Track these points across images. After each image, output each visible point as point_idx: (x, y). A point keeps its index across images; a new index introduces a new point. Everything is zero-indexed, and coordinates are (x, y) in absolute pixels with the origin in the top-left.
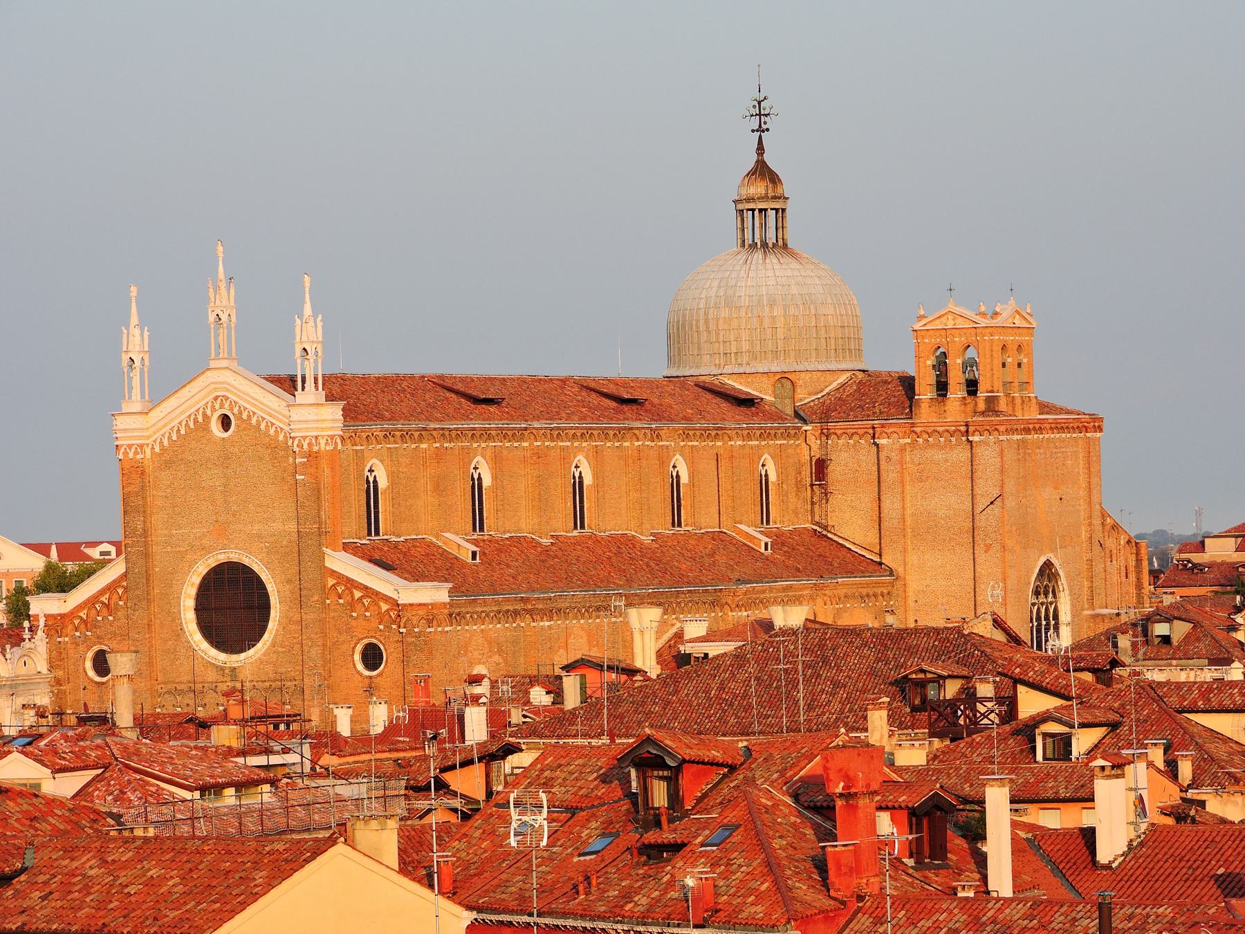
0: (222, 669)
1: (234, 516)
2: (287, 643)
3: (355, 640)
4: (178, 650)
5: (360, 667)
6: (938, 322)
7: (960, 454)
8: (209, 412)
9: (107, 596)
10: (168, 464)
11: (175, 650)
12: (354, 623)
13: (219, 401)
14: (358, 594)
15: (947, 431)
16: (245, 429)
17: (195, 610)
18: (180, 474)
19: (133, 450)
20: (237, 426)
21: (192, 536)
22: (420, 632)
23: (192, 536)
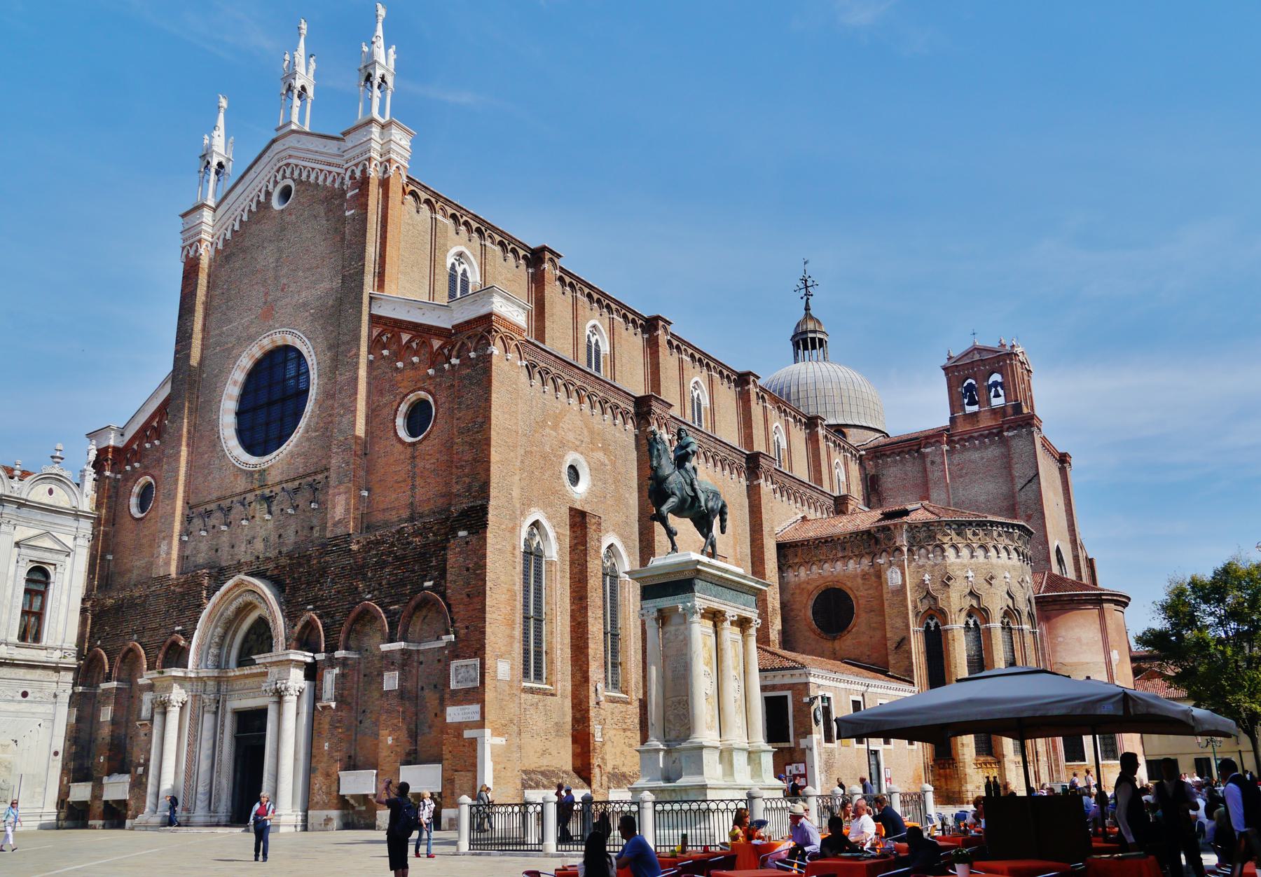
0: (251, 474)
1: (282, 290)
2: (322, 425)
3: (398, 400)
4: (212, 463)
5: (403, 434)
6: (965, 358)
7: (993, 452)
8: (271, 187)
9: (157, 420)
10: (228, 258)
11: (210, 464)
12: (399, 377)
13: (281, 172)
15: (981, 435)
17: (236, 414)
18: (237, 265)
20: (297, 191)
21: (240, 327)
23: (240, 327)
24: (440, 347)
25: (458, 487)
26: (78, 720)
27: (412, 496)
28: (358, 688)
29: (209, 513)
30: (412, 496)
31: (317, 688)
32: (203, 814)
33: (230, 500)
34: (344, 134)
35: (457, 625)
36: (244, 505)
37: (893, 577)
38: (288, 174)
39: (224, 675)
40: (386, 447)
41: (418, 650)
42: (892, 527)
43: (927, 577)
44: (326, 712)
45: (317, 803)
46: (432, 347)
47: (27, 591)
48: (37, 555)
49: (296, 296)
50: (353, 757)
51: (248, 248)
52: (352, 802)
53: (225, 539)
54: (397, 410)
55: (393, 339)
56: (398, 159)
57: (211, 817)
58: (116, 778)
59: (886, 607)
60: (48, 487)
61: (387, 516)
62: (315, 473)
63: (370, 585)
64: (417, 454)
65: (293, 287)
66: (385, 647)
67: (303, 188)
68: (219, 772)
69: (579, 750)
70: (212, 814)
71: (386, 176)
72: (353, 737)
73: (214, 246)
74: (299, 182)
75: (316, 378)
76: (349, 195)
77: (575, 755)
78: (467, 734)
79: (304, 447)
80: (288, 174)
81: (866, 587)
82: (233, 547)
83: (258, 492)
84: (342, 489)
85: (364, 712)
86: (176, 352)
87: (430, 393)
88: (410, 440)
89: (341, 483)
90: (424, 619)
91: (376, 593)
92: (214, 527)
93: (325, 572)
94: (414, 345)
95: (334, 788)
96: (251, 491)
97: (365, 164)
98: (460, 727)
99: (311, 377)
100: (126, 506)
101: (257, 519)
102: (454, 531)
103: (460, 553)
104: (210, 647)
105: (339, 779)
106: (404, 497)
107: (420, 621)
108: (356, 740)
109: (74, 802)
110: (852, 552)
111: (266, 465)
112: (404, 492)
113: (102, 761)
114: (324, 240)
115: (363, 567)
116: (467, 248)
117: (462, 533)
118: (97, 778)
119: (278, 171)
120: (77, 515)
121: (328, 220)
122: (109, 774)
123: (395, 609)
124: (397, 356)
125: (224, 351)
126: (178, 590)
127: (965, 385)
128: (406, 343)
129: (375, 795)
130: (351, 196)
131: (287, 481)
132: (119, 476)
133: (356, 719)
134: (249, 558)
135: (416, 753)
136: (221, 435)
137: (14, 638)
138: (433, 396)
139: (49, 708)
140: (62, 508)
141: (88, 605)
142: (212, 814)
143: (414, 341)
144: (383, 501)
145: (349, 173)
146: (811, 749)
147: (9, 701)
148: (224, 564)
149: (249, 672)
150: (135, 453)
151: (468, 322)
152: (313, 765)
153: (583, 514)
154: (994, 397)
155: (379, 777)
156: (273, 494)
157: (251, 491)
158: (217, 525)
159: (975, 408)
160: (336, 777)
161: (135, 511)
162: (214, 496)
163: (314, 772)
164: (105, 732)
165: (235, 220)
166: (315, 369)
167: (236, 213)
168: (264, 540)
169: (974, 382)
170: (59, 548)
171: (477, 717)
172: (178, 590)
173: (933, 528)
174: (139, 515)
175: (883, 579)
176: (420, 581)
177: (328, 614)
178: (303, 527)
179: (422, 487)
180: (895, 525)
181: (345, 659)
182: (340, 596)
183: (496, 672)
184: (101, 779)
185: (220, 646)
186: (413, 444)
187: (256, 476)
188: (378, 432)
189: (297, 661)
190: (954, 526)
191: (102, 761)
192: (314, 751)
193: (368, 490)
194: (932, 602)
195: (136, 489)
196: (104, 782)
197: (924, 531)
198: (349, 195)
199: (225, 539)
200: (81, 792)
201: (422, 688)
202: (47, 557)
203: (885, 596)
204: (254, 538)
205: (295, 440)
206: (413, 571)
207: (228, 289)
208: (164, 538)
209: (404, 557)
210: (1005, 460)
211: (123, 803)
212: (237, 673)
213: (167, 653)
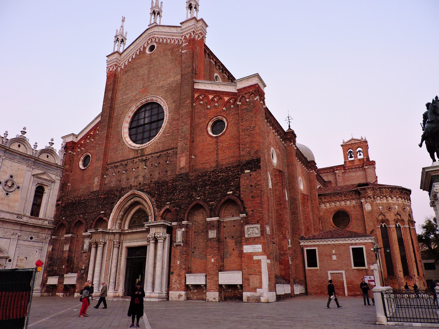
0: (136, 151)
1: (151, 82)
3: (208, 121)
5: (211, 133)
8: (145, 45)
9: (93, 132)
10: (126, 72)
11: (117, 147)
12: (208, 111)
13: (150, 40)
14: (211, 97)
16: (160, 47)
18: (130, 74)
19: (112, 68)
20: (157, 47)
21: (132, 96)
22: (250, 102)
23: (132, 96)
24: (229, 99)
25: (243, 153)
26: (53, 249)
27: (217, 158)
28: (192, 237)
29: (116, 167)
30: (217, 158)
31: (173, 237)
32: (112, 291)
33: (126, 161)
34: (181, 24)
35: (247, 210)
36: (133, 163)
37: (368, 207)
38: (153, 40)
39: (123, 232)
40: (203, 139)
41: (223, 221)
42: (367, 189)
43: (381, 207)
44: (178, 248)
45: (174, 288)
46: (224, 99)
47: (35, 196)
48: (40, 181)
49: (158, 84)
50: (190, 268)
51: (135, 68)
52: (192, 288)
53: (124, 176)
54: (208, 124)
55: (205, 97)
56: (203, 34)
57: (115, 293)
58: (70, 275)
59: (365, 218)
60: (47, 154)
61: (204, 166)
62: (168, 150)
63: (199, 193)
64: (219, 141)
65: (156, 81)
66: (208, 219)
67: (160, 45)
68: (119, 273)
69: (283, 267)
70: (116, 292)
71: (199, 39)
72: (190, 259)
73: (120, 68)
74: (158, 43)
75: (168, 114)
76: (184, 45)
77: (281, 269)
78: (255, 258)
79: (163, 140)
80: (153, 40)
81: (355, 211)
82: (128, 180)
83: (139, 158)
84: (184, 154)
85: (195, 248)
86: (103, 106)
87: (224, 117)
88: (215, 136)
89: (183, 152)
90: (226, 208)
91: (202, 197)
92: (119, 172)
93: (176, 188)
94: (216, 99)
95: (183, 281)
96: (136, 158)
97: (191, 34)
98: (250, 255)
99: (165, 113)
100: (78, 164)
101: (140, 168)
102: (243, 171)
103: (247, 179)
104: (117, 220)
105: (186, 277)
106: (213, 158)
107: (224, 209)
108: (191, 260)
109: (49, 285)
110: (349, 198)
111: (144, 147)
112: (213, 156)
113: (64, 267)
114: (170, 63)
115: (195, 186)
116: (219, 75)
117: (247, 171)
118: (61, 275)
119: (149, 40)
120: (57, 166)
121: (172, 56)
122: (66, 273)
123: (213, 203)
124: (207, 104)
125: (124, 105)
126: (102, 196)
127: (349, 151)
128: (211, 99)
129: (205, 285)
130: (185, 46)
131: (154, 153)
132: (74, 153)
133: (191, 252)
134: (136, 184)
135: (224, 266)
136: (123, 136)
137: (29, 214)
138: (226, 118)
139: (40, 245)
140: (51, 163)
141: (60, 202)
142: (116, 292)
143: (215, 98)
144: (202, 160)
145: (183, 37)
146: (376, 270)
147: (25, 240)
148: (123, 186)
149: (136, 231)
150: (82, 145)
151: (245, 88)
152: (171, 271)
153: (280, 171)
154: (359, 155)
155: (208, 277)
156: (147, 158)
157: (136, 158)
158: (120, 171)
159: (353, 159)
160: (184, 277)
161: (81, 167)
162: (120, 159)
163: (172, 273)
164: (66, 255)
165: (129, 58)
166: (168, 111)
167: (130, 56)
168: (143, 176)
169: (352, 150)
170: (49, 179)
171: (261, 250)
172: (102, 196)
173: (381, 190)
174: (83, 168)
175: (363, 208)
176: (225, 192)
177: (177, 206)
178: (162, 171)
179: (222, 154)
180: (368, 188)
181: (187, 225)
182: (183, 198)
183: (266, 230)
184: (63, 275)
185: (122, 220)
186: (215, 137)
187: (139, 152)
188: (199, 133)
189: (165, 225)
190: (390, 189)
191: (64, 267)
192: (172, 264)
193: (195, 156)
194: (383, 217)
195: (82, 158)
196: (64, 276)
197: (379, 191)
198: (184, 45)
199: (124, 176)
200: (53, 281)
201: (226, 238)
202: (45, 183)
203: (365, 214)
204: (138, 176)
205: (158, 137)
206: (221, 187)
207: (126, 83)
208: (96, 176)
209: (217, 181)
210: (364, 176)
211: (73, 286)
212: (130, 231)
213: (97, 222)
